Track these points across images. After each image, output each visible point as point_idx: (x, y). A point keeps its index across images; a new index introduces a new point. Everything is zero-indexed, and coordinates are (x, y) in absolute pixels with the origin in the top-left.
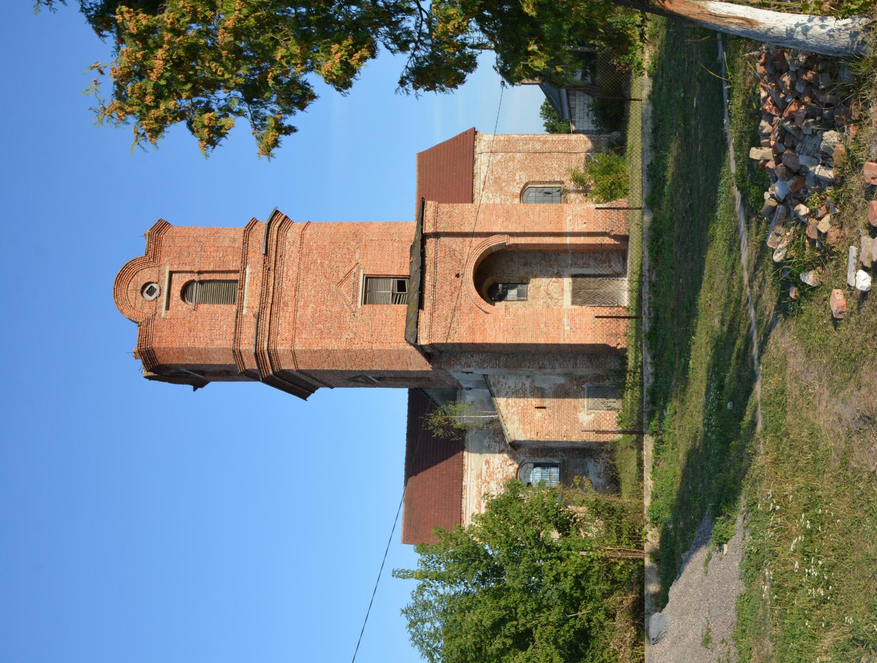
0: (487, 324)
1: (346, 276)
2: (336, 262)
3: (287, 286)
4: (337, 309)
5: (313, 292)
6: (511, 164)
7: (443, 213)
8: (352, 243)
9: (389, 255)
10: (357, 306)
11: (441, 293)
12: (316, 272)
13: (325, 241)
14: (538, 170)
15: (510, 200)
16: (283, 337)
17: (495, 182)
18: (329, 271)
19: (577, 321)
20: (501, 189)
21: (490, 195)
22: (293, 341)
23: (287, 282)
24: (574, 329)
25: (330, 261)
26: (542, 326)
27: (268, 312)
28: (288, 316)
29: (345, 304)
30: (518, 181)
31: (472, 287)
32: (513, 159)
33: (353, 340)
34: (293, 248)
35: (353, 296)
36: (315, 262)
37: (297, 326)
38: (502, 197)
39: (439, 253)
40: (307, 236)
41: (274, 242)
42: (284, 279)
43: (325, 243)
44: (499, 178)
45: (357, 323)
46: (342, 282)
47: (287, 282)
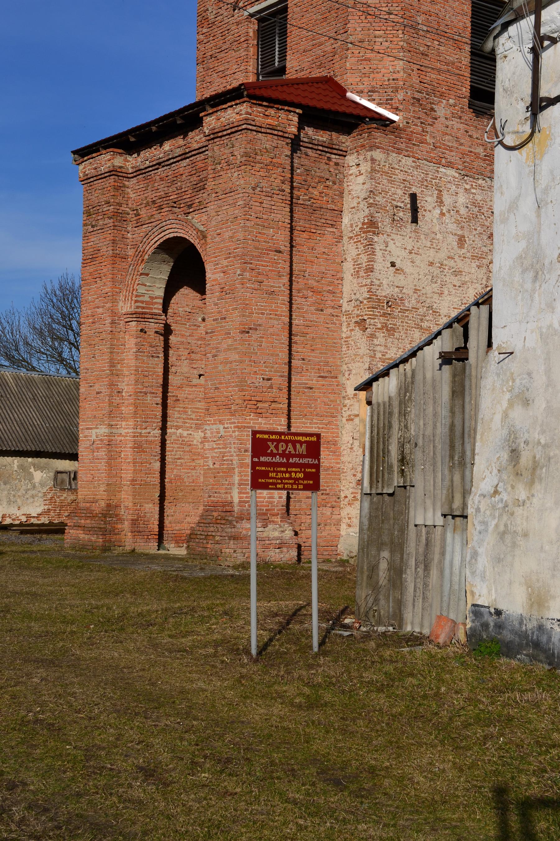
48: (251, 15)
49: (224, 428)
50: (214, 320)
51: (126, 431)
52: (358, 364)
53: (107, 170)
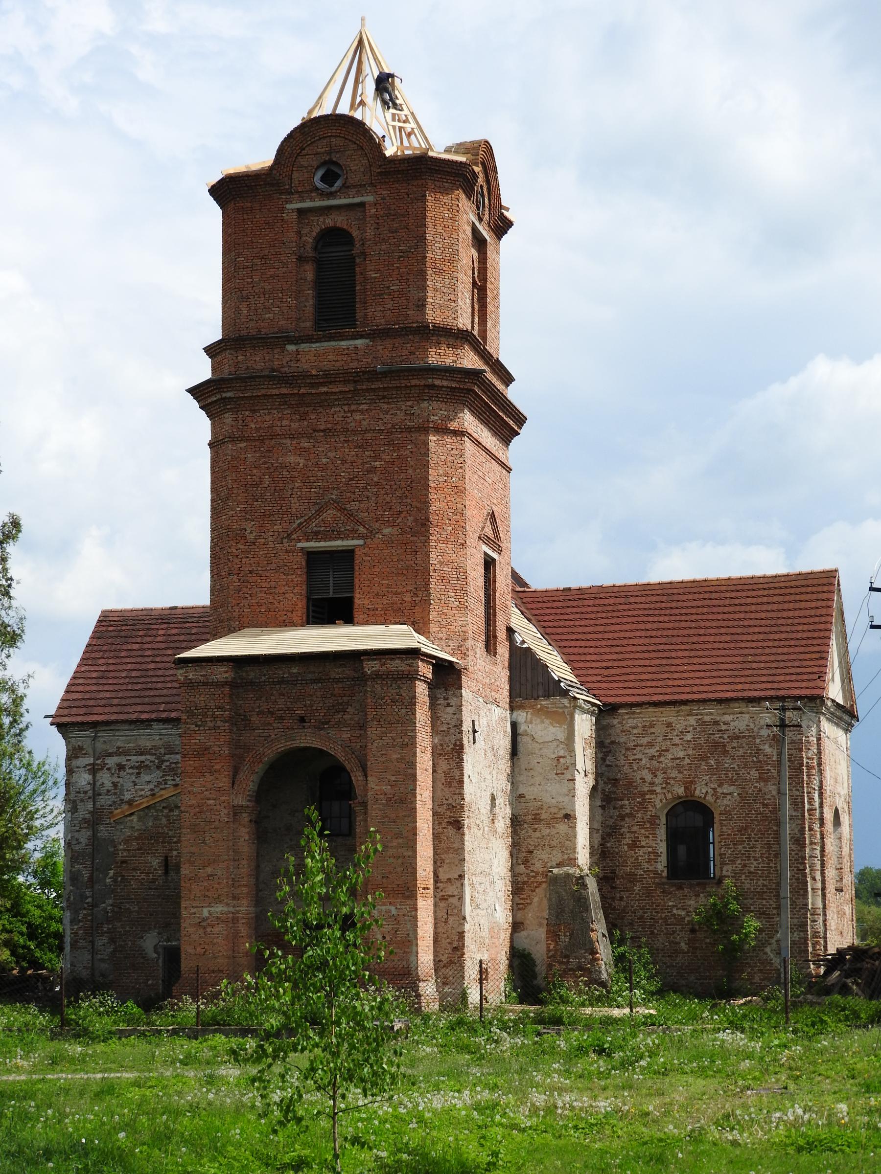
0: (212, 778)
1: (350, 515)
2: (377, 495)
3: (337, 413)
4: (295, 506)
5: (324, 461)
6: (754, 774)
7: (399, 688)
8: (411, 519)
9: (389, 586)
10: (300, 541)
11: (272, 694)
12: (360, 461)
13: (415, 470)
14: (742, 830)
15: (681, 776)
16: (249, 419)
17: (716, 745)
18: (362, 483)
19: (216, 929)
20: (704, 758)
21: (689, 737)
22: (242, 439)
23: (342, 414)
24: (204, 924)
25: (377, 484)
26: (209, 870)
27: (284, 391)
28: (285, 423)
29: (302, 520)
30: (719, 790)
31: (282, 746)
32: (764, 778)
33: (242, 541)
34: (401, 415)
35: (317, 533)
36: (377, 458)
37: (267, 442)
38: (687, 761)
39: (340, 685)
40: (422, 437)
41: (404, 383)
42: (346, 408)
43: (410, 471)
44: (725, 752)
45: (271, 545)
46: (342, 510)
47: (342, 414)
48: (302, 548)
49: (396, 908)
50: (379, 822)
51: (238, 909)
52: (451, 856)
53: (222, 680)
